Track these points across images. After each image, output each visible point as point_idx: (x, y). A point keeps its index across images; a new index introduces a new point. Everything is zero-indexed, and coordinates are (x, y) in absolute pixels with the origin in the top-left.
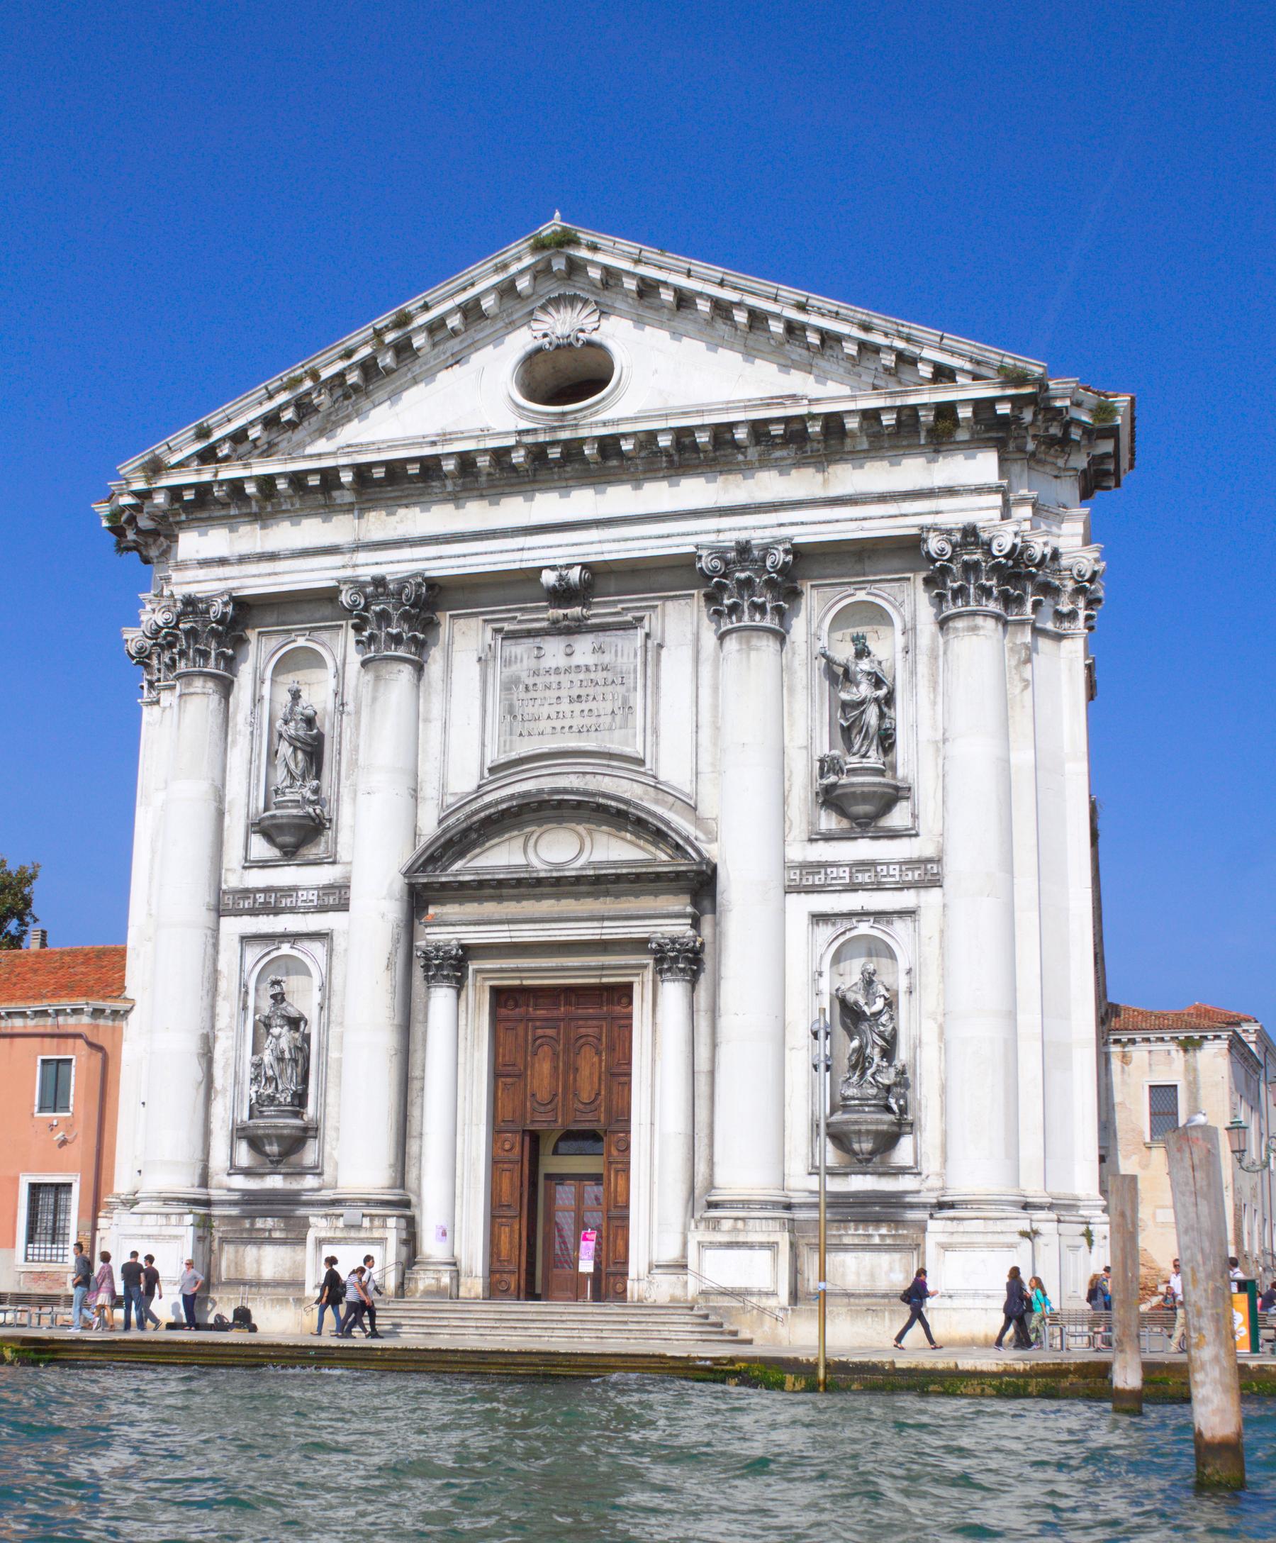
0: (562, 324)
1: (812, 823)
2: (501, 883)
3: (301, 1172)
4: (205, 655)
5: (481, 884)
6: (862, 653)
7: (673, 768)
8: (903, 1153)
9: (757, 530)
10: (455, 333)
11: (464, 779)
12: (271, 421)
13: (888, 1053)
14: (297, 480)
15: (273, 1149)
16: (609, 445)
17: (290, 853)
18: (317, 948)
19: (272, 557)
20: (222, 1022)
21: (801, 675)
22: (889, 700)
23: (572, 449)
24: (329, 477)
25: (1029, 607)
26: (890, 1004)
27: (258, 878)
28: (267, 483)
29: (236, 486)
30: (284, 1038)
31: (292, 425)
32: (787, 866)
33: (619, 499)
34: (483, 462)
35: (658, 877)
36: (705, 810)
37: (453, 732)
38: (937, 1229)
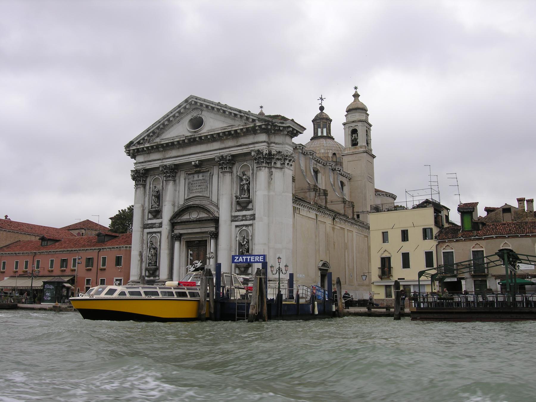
0: (195, 114)
1: (236, 208)
2: (185, 222)
3: (155, 276)
4: (140, 180)
5: (181, 222)
6: (244, 175)
7: (214, 199)
8: (250, 271)
9: (225, 152)
10: (178, 117)
11: (182, 202)
12: (148, 136)
14: (152, 147)
15: (151, 272)
16: (200, 138)
17: (155, 217)
18: (159, 234)
19: (150, 161)
20: (144, 248)
21: (235, 179)
22: (249, 183)
23: (194, 139)
25: (273, 164)
26: (248, 242)
27: (150, 222)
28: (147, 148)
29: (143, 148)
30: (153, 251)
31: (152, 136)
32: (232, 216)
34: (181, 142)
35: (209, 220)
37: (180, 193)
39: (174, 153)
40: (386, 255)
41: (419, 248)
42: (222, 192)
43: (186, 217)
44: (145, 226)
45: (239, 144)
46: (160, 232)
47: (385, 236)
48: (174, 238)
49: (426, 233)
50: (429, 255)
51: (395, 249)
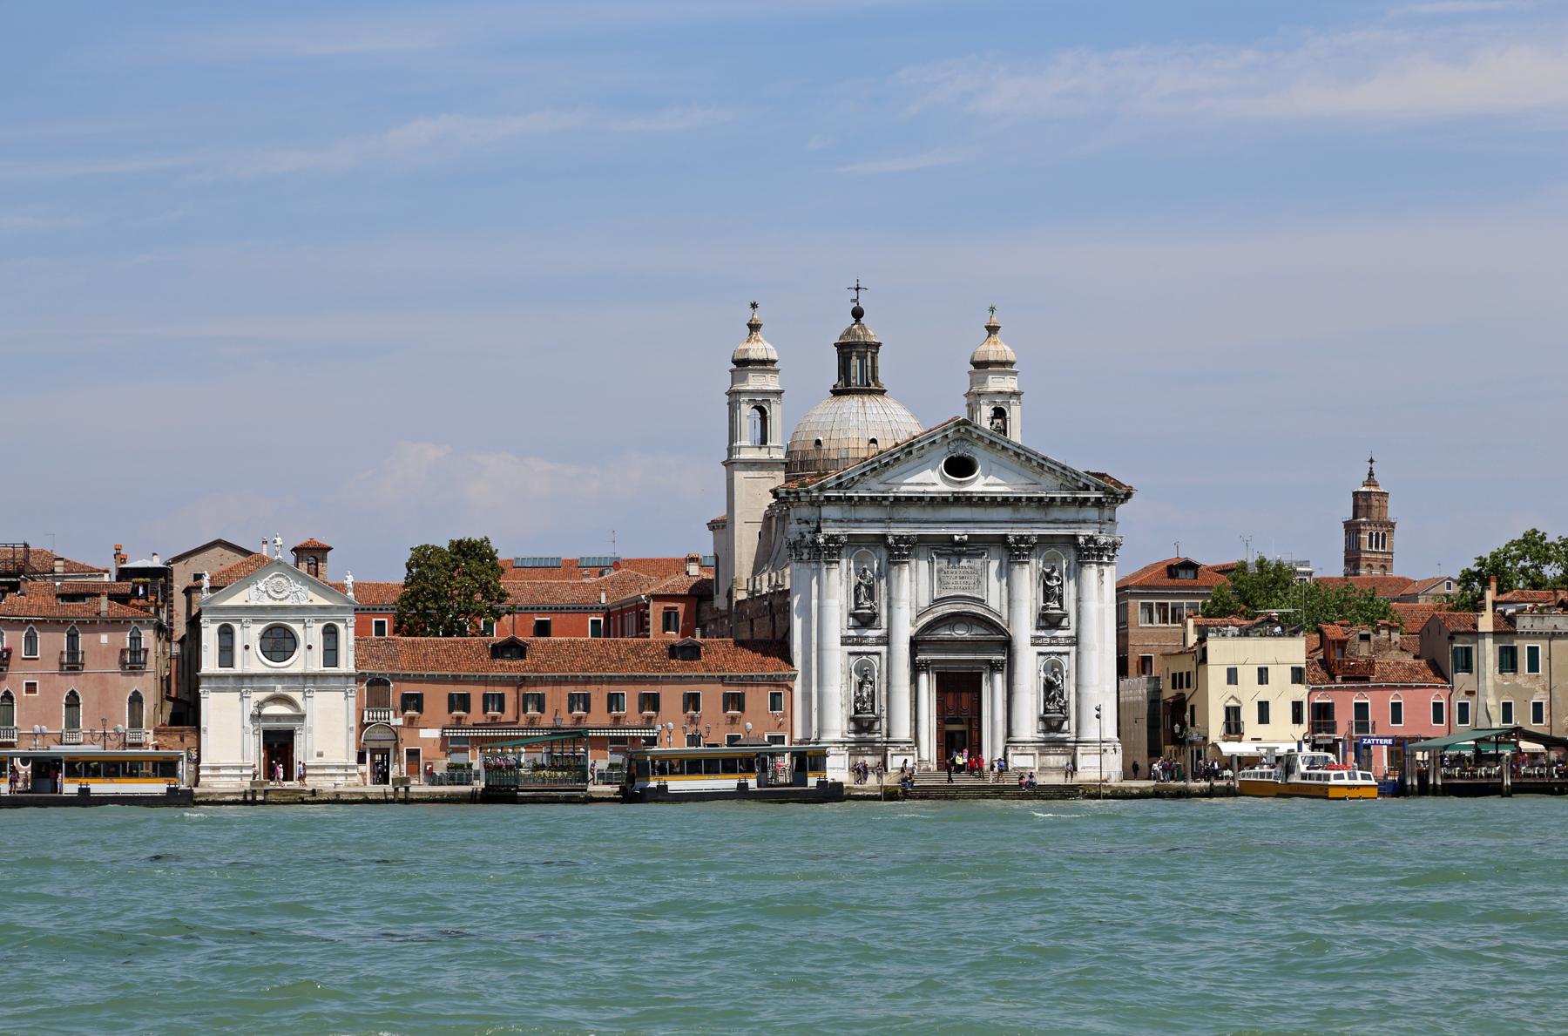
7: (994, 603)
8: (1065, 726)
13: (1061, 696)
18: (876, 658)
24: (885, 498)
27: (852, 633)
29: (851, 498)
33: (978, 513)
36: (1005, 617)
38: (1080, 750)
39: (913, 513)
40: (1232, 703)
41: (1283, 693)
42: (1015, 597)
43: (945, 633)
44: (846, 641)
45: (1050, 518)
46: (878, 654)
47: (1232, 676)
48: (916, 669)
49: (1297, 675)
50: (1297, 706)
51: (1248, 694)
